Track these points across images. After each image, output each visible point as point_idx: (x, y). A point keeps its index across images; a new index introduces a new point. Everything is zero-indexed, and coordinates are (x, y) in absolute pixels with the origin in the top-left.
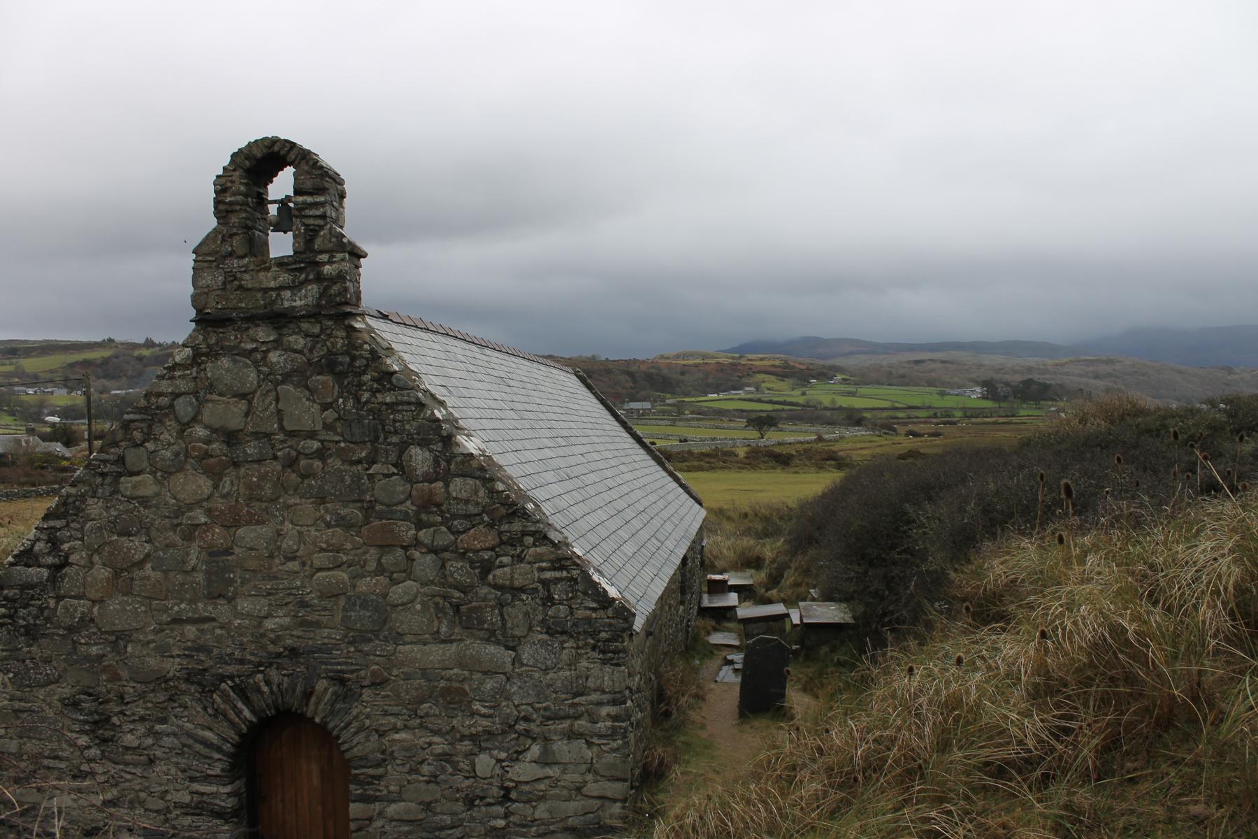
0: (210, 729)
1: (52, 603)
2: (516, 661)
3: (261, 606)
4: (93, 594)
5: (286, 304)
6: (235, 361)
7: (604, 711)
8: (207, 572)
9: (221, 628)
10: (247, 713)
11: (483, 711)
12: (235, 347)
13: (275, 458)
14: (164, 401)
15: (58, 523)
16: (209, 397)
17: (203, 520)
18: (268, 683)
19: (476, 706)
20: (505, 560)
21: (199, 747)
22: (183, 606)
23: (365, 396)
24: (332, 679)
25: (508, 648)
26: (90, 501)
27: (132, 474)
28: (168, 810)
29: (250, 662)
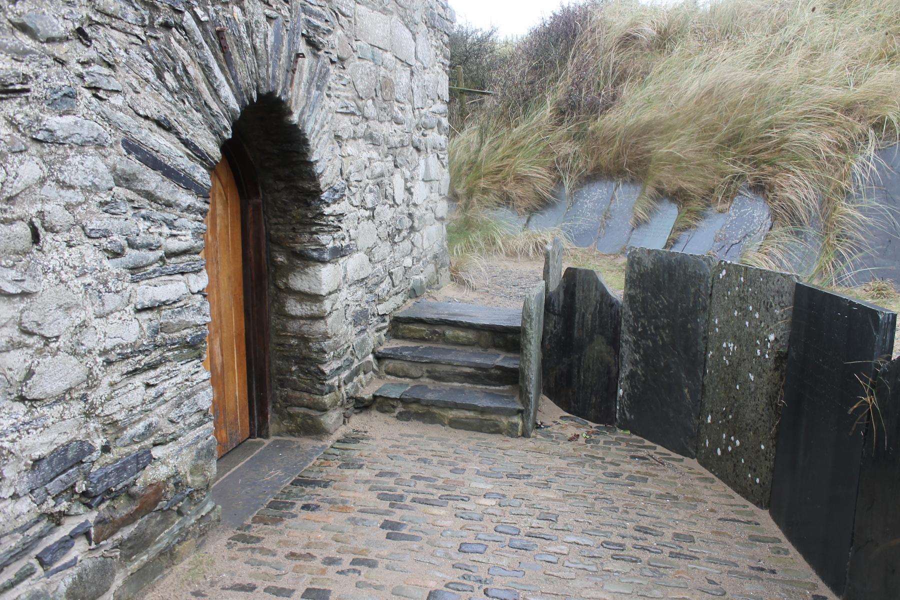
0: (164, 125)
10: (226, 92)
21: (153, 180)
28: (91, 381)
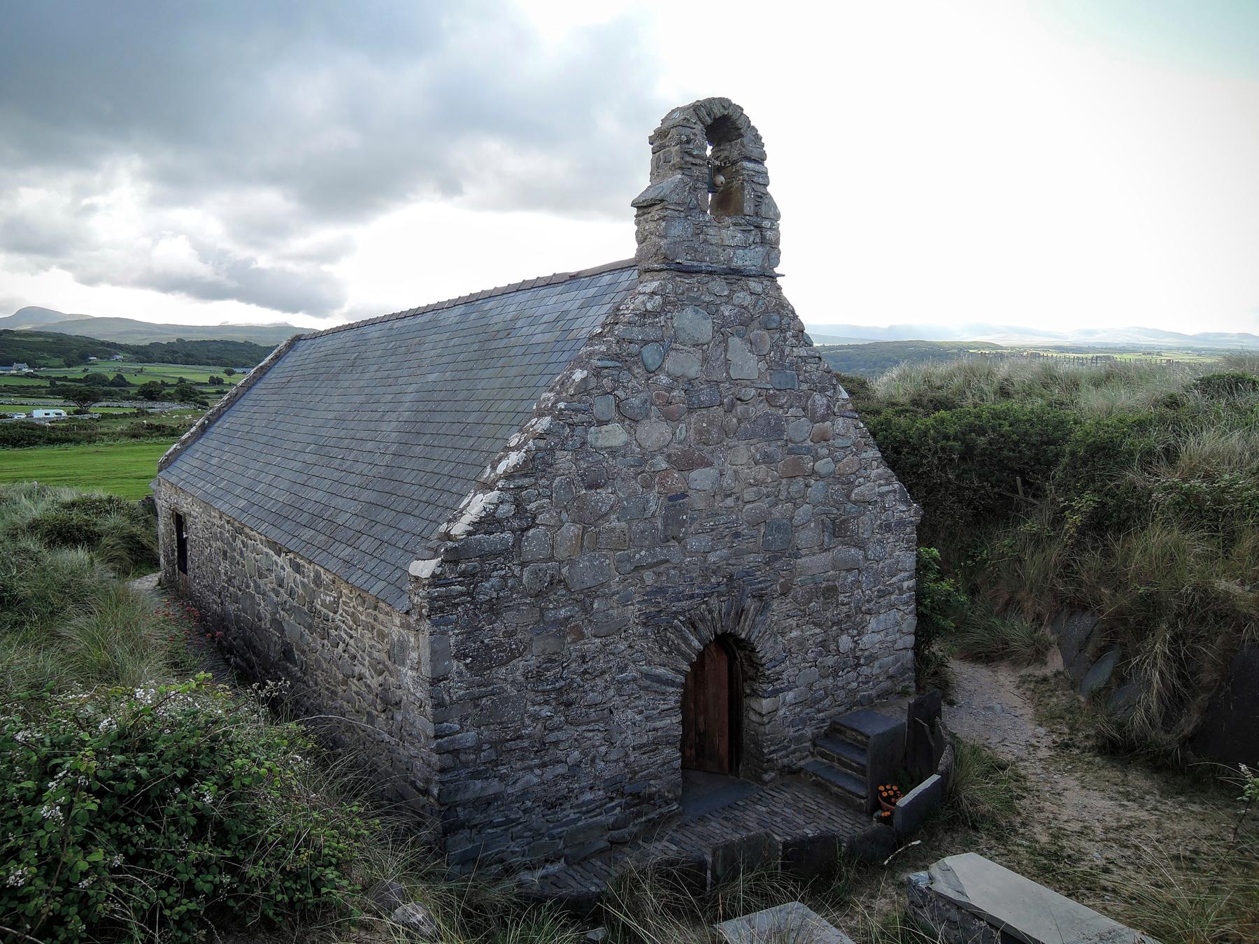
1: (517, 570)
2: (866, 558)
3: (705, 541)
4: (561, 553)
5: (740, 263)
6: (697, 312)
7: (905, 585)
8: (665, 518)
9: (674, 568)
10: (696, 643)
11: (846, 600)
12: (697, 298)
13: (722, 404)
14: (634, 348)
15: (526, 481)
16: (673, 345)
17: (664, 465)
18: (710, 612)
19: (841, 598)
20: (861, 480)
22: (643, 553)
23: (787, 350)
24: (754, 597)
25: (860, 548)
26: (559, 454)
27: (601, 423)
29: (698, 595)
